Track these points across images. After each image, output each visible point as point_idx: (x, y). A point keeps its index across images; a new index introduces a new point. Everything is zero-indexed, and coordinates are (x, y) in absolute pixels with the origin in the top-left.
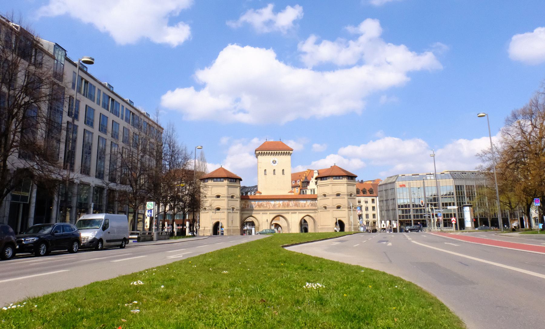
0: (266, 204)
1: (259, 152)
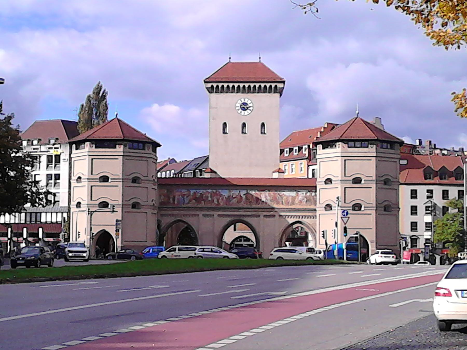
0: (211, 197)
1: (212, 86)
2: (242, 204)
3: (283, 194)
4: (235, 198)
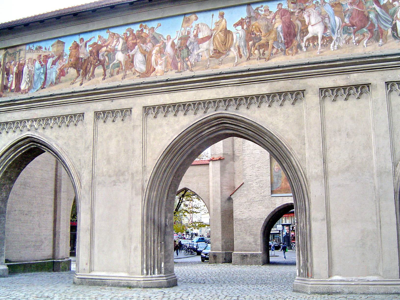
0: (126, 49)
2: (234, 58)
4: (203, 40)
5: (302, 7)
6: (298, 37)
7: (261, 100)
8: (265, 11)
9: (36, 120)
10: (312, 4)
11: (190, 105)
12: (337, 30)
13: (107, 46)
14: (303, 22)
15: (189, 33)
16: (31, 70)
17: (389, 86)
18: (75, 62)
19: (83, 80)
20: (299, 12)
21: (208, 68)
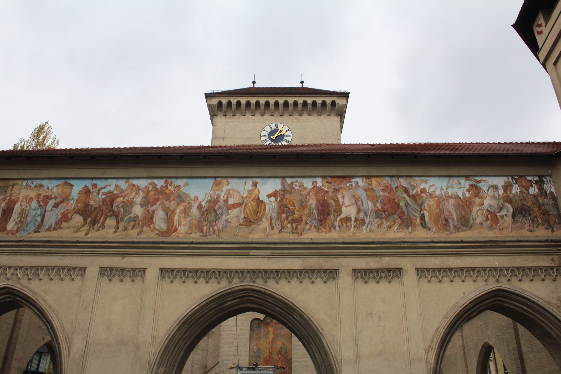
0: (145, 204)
1: (220, 104)
3: (423, 191)
4: (234, 206)
5: (336, 188)
6: (332, 216)
7: (293, 275)
8: (300, 186)
9: (21, 268)
10: (346, 186)
11: (214, 272)
12: (369, 213)
13: (124, 197)
14: (337, 202)
15: (218, 197)
16: (25, 209)
17: (419, 272)
18: (82, 208)
19: (89, 229)
20: (333, 192)
21: (237, 235)
